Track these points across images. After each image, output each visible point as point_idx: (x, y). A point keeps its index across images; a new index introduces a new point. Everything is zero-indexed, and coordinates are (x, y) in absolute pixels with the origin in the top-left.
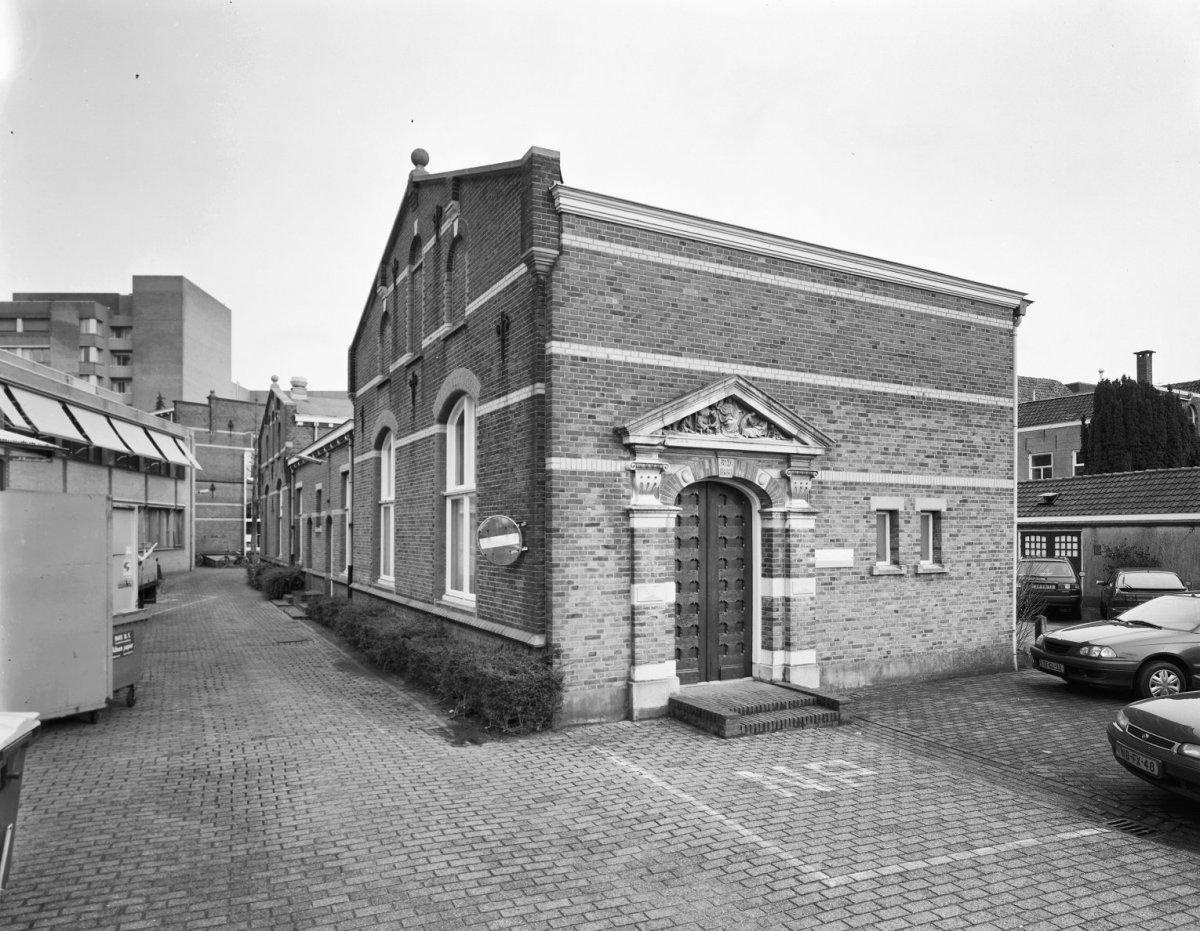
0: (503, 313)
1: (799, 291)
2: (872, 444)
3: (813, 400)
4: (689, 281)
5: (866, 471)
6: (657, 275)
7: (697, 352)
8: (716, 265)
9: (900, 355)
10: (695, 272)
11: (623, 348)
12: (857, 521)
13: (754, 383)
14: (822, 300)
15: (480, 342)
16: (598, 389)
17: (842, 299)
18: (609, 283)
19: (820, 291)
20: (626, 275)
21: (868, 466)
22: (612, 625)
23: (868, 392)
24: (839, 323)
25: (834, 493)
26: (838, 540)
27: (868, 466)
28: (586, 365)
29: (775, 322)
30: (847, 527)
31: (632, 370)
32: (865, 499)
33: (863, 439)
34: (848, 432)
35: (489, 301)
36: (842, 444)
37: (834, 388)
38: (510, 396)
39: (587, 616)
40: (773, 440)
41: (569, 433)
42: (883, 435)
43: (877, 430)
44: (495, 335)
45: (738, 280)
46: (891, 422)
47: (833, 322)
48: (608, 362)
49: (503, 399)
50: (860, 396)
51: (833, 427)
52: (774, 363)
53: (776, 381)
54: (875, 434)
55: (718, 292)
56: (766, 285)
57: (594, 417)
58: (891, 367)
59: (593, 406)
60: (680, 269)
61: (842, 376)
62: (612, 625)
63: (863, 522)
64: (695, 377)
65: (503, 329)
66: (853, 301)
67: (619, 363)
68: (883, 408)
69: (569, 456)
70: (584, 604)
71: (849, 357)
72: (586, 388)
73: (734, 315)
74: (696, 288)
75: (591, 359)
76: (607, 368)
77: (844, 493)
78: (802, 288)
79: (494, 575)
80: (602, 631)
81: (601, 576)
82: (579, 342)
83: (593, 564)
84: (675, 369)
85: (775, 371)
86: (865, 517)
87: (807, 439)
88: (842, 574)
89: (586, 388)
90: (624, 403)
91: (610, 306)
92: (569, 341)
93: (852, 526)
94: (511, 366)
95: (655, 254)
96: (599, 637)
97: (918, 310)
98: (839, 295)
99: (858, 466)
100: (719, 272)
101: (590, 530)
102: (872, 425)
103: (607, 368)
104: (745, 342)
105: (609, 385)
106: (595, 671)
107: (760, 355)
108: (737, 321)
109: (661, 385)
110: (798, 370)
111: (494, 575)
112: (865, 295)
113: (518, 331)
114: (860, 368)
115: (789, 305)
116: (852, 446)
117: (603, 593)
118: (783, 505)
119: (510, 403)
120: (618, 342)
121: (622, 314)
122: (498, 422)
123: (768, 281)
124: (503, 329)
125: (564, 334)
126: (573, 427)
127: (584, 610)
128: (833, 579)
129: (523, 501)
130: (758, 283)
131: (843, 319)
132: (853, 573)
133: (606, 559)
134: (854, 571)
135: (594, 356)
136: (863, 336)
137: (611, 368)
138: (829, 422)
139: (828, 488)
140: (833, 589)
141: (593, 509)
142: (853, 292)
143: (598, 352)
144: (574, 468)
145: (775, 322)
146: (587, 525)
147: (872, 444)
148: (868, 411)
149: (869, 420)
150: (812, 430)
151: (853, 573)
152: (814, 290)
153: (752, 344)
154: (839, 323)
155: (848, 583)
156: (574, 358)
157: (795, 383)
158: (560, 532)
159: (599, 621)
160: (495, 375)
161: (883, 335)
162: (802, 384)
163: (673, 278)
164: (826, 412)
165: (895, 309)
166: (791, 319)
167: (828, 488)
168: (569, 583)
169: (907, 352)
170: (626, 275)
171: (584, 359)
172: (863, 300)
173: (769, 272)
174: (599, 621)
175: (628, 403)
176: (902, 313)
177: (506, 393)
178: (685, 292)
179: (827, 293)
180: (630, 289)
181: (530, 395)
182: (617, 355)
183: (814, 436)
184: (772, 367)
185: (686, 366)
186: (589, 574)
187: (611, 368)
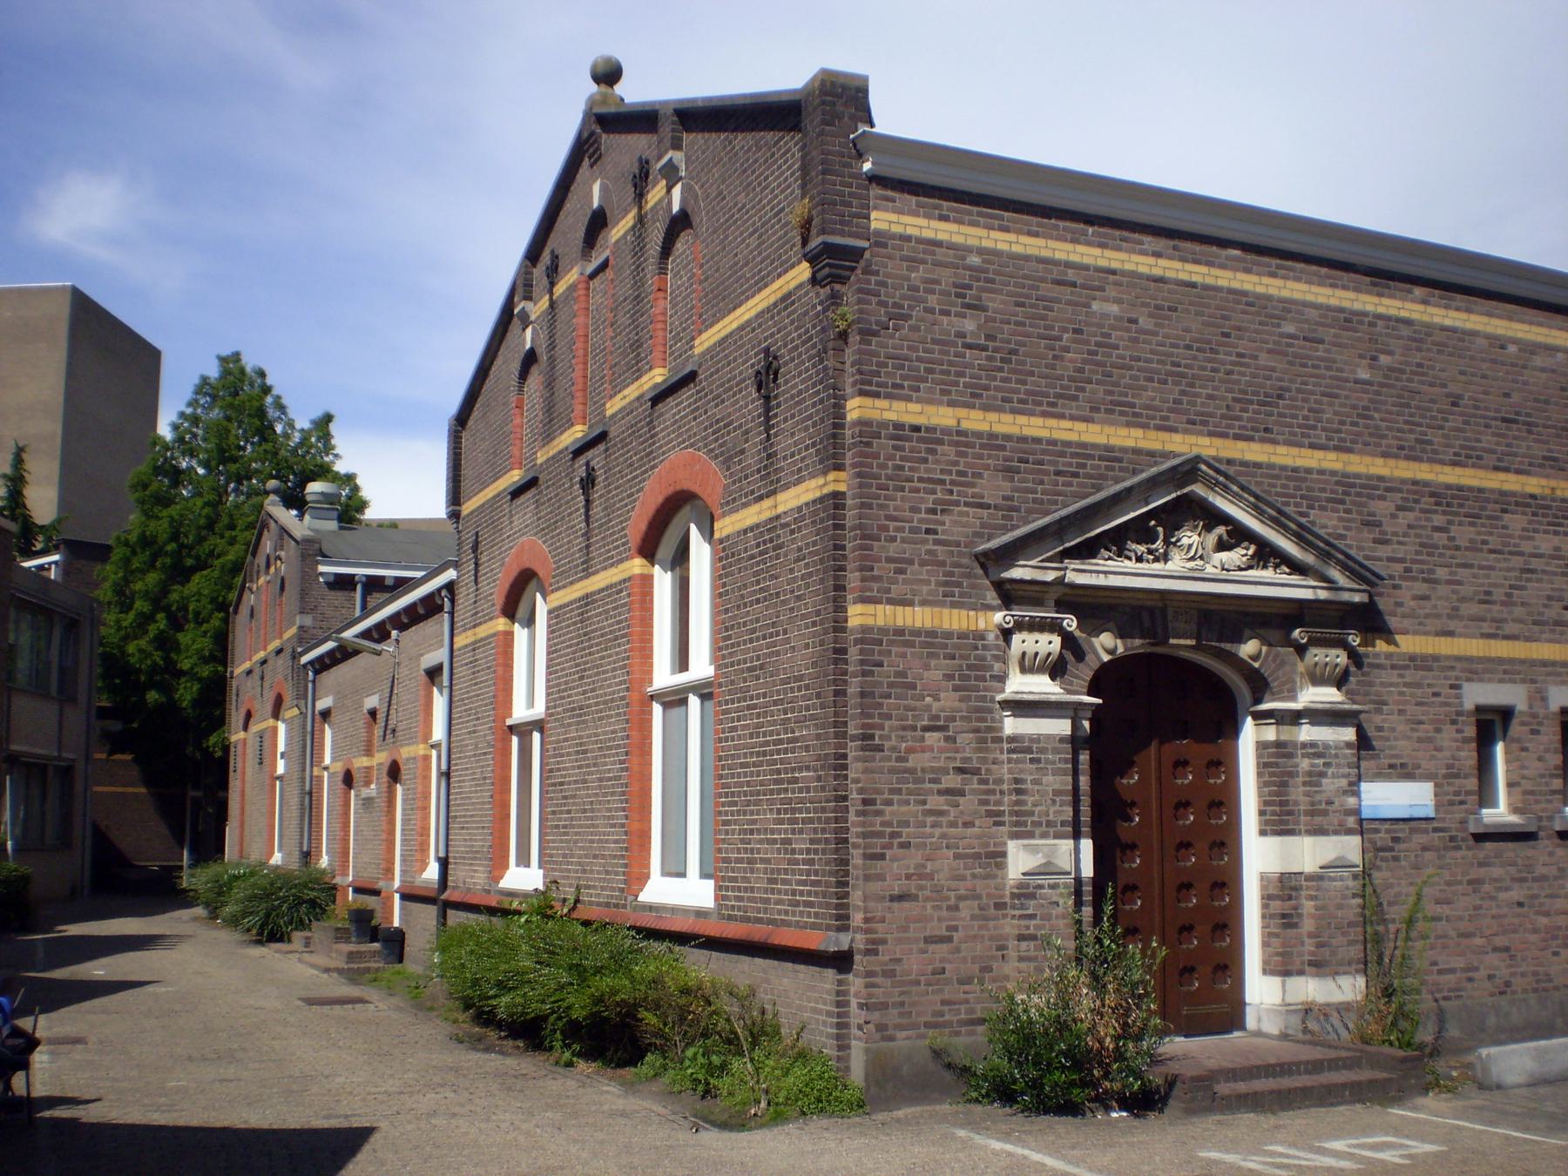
0: (767, 351)
1: (1306, 304)
2: (1459, 583)
3: (1342, 502)
4: (1102, 289)
5: (1451, 634)
6: (1043, 280)
7: (1122, 414)
8: (1151, 260)
9: (1504, 420)
10: (1114, 272)
11: (986, 408)
12: (1438, 730)
13: (1231, 471)
14: (1349, 320)
15: (723, 402)
16: (942, 482)
17: (1388, 318)
18: (958, 295)
19: (1346, 304)
20: (988, 280)
21: (1452, 625)
22: (973, 917)
23: (1449, 487)
24: (1384, 359)
25: (1392, 676)
26: (1403, 765)
27: (1452, 625)
28: (920, 440)
29: (1264, 359)
30: (1420, 740)
31: (1003, 448)
32: (1452, 687)
33: (1441, 573)
34: (1414, 561)
35: (741, 328)
36: (1404, 584)
37: (1381, 478)
38: (781, 497)
39: (927, 899)
40: (1268, 574)
41: (890, 560)
42: (1481, 567)
43: (1470, 557)
44: (753, 390)
45: (1193, 285)
46: (1493, 541)
47: (1374, 359)
48: (959, 433)
49: (767, 503)
50: (1432, 495)
51: (1384, 551)
52: (1266, 435)
53: (1271, 466)
54: (1465, 566)
55: (1157, 307)
56: (1244, 293)
57: (935, 532)
58: (1487, 440)
59: (933, 511)
60: (1086, 268)
61: (1396, 457)
62: (973, 917)
63: (1449, 732)
64: (1120, 460)
65: (767, 377)
66: (1408, 322)
67: (979, 435)
68: (1478, 517)
69: (891, 602)
70: (921, 876)
71: (1407, 422)
72: (921, 480)
73: (1188, 347)
74: (1119, 301)
75: (928, 429)
76: (957, 444)
77: (1410, 675)
78: (1310, 298)
79: (752, 832)
80: (955, 929)
81: (953, 824)
82: (908, 399)
83: (935, 802)
84: (1084, 445)
85: (1268, 448)
86: (1454, 722)
87: (1336, 574)
88: (1412, 831)
89: (921, 480)
90: (988, 507)
91: (961, 335)
92: (889, 396)
93: (1430, 740)
94: (783, 444)
95: (1040, 242)
96: (949, 939)
97: (1530, 337)
98: (1381, 310)
99: (1437, 624)
100: (1157, 272)
101: (933, 738)
102: (1457, 548)
103: (957, 444)
104: (1210, 397)
105: (961, 473)
106: (943, 1003)
107: (1238, 418)
108: (1195, 358)
109: (1058, 473)
110: (1313, 446)
111: (752, 832)
112: (1431, 310)
113: (795, 382)
114: (1430, 442)
115: (1289, 328)
116: (1421, 588)
117: (957, 856)
118: (1294, 698)
119: (781, 509)
120: (975, 398)
121: (985, 349)
122: (758, 545)
123: (1247, 287)
124: (767, 377)
125: (879, 385)
126: (893, 549)
127: (922, 888)
128: (1396, 840)
129: (807, 687)
130: (1231, 291)
131: (1390, 353)
132: (1436, 830)
133: (961, 793)
134: (1435, 824)
135: (934, 421)
136: (1432, 385)
137: (967, 445)
138: (1375, 541)
139: (1379, 666)
140: (1396, 859)
141: (937, 699)
142: (1409, 305)
143: (943, 416)
144: (900, 623)
145: (1264, 359)
146: (926, 729)
147: (1459, 583)
148: (1450, 522)
149: (1452, 539)
150: (1340, 556)
151: (1436, 830)
152: (1333, 302)
153: (1224, 399)
154: (1384, 359)
155: (1424, 849)
156: (899, 426)
157: (1308, 471)
158: (877, 741)
159: (949, 908)
160: (752, 460)
161: (1470, 383)
162: (1321, 472)
163: (1074, 285)
164: (1367, 524)
165: (1488, 337)
166: (1296, 356)
167: (1379, 666)
168: (893, 835)
169: (1517, 414)
170: (988, 280)
171: (916, 429)
172: (1426, 318)
173: (1247, 271)
174: (949, 908)
175: (996, 507)
176: (1500, 343)
177: (773, 493)
178: (1095, 306)
179: (1357, 306)
180: (994, 303)
181: (818, 494)
182: (976, 421)
183: (1345, 568)
184: (1263, 440)
185: (1102, 440)
186: (930, 820)
187: (967, 445)
